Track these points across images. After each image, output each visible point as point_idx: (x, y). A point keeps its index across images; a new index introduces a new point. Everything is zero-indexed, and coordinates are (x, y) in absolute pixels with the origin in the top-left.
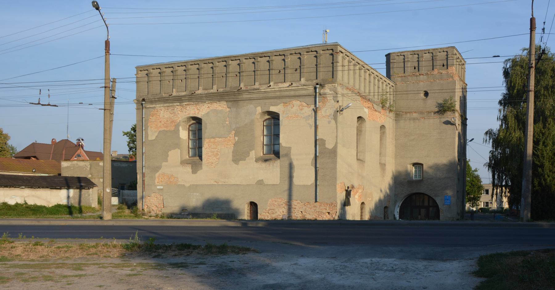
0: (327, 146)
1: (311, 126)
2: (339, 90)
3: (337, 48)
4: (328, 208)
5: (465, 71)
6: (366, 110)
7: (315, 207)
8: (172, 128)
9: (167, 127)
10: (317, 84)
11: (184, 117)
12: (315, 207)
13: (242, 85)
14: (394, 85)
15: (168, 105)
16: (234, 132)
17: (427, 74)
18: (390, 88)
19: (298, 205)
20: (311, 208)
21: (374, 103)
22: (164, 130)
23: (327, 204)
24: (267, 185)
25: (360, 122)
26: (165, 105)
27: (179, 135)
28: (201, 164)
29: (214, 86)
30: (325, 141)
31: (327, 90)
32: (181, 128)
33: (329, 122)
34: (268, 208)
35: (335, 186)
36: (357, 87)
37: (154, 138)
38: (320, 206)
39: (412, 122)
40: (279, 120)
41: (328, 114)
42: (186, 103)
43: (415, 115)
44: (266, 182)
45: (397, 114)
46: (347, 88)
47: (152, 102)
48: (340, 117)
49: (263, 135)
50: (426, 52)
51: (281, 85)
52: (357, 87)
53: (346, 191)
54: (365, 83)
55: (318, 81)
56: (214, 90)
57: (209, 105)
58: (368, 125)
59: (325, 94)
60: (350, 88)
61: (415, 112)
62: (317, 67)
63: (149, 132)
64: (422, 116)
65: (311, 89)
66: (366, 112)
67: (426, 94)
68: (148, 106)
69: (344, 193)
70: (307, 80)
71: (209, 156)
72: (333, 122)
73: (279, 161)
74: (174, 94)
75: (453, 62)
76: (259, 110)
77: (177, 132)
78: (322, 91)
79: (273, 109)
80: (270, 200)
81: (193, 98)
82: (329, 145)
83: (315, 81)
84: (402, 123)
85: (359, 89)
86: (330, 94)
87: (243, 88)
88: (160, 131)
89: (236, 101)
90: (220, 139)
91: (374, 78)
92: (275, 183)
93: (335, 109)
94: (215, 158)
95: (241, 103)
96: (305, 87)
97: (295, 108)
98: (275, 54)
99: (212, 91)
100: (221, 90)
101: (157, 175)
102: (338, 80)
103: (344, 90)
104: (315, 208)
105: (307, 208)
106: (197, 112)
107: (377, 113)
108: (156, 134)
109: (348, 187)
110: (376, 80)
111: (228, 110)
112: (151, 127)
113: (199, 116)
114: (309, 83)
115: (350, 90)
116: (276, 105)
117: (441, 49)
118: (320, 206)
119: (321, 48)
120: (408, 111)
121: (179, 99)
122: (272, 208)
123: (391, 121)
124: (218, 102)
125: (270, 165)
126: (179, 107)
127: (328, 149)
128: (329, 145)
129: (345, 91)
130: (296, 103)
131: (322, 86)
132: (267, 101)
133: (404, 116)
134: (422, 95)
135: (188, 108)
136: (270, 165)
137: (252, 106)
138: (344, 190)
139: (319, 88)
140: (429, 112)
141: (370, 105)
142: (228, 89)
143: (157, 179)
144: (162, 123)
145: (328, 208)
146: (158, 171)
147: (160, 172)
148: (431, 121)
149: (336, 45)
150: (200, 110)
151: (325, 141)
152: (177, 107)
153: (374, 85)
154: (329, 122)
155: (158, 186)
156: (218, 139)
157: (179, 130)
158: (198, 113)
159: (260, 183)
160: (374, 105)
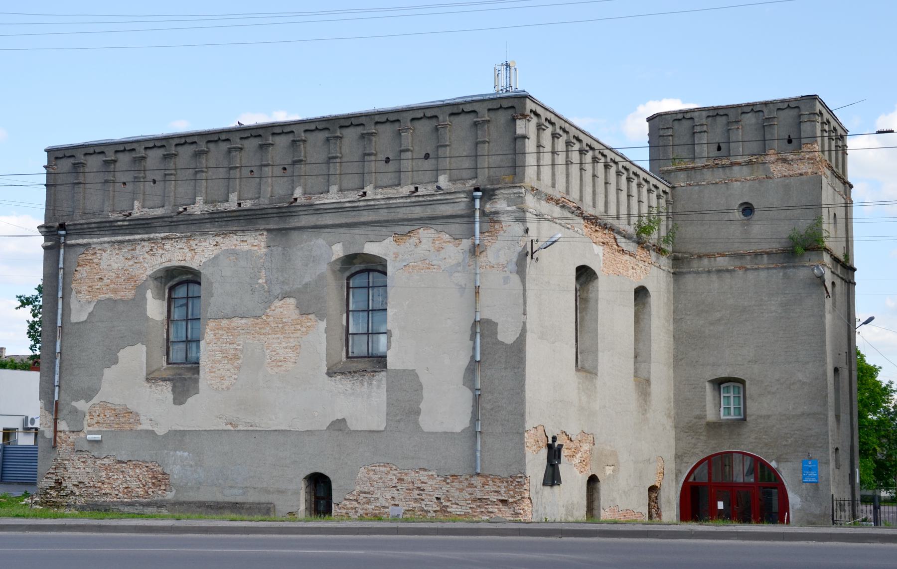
0: (501, 337)
1: (462, 288)
2: (530, 202)
3: (525, 104)
4: (503, 490)
5: (845, 153)
6: (599, 250)
7: (471, 485)
8: (130, 295)
9: (115, 291)
10: (477, 190)
11: (158, 267)
12: (471, 485)
13: (298, 193)
14: (668, 190)
15: (120, 238)
17: (749, 163)
18: (659, 197)
19: (430, 482)
21: (619, 233)
22: (109, 299)
23: (501, 480)
25: (583, 279)
26: (113, 239)
27: (145, 309)
28: (196, 381)
29: (231, 196)
30: (497, 324)
31: (501, 205)
32: (149, 294)
33: (506, 280)
34: (358, 489)
35: (521, 435)
36: (575, 194)
37: (85, 318)
38: (484, 484)
39: (714, 277)
40: (385, 273)
41: (503, 260)
42: (162, 235)
43: (722, 262)
44: (353, 425)
45: (677, 260)
46: (550, 199)
47: (81, 233)
48: (531, 268)
49: (348, 312)
50: (745, 110)
51: (391, 192)
52: (575, 194)
53: (550, 447)
54: (594, 186)
55: (482, 181)
56: (232, 205)
57: (218, 239)
58: (603, 286)
59: (496, 213)
60: (558, 196)
61: (724, 256)
62: (477, 146)
63: (74, 305)
64: (738, 263)
65: (463, 198)
66: (596, 255)
67: (748, 209)
68: (73, 242)
69: (544, 452)
70: (451, 180)
72: (515, 278)
73: (384, 373)
74: (138, 211)
75: (814, 131)
76: (339, 251)
77: (139, 301)
78: (488, 207)
79: (371, 249)
81: (181, 223)
82: (507, 336)
83: (470, 184)
84: (689, 281)
85: (581, 200)
86: (508, 212)
87: (301, 201)
88: (99, 301)
89: (283, 231)
90: (244, 321)
91: (619, 174)
93: (519, 249)
94: (229, 366)
95: (295, 235)
96: (448, 197)
97: (424, 246)
98: (377, 118)
99: (224, 206)
100: (247, 205)
102: (527, 180)
103: (543, 203)
104: (470, 490)
105: (453, 490)
106: (189, 255)
107: (627, 257)
108: (91, 308)
109: (554, 439)
110: (624, 177)
111: (264, 251)
112: (79, 292)
113: (194, 265)
114: (459, 186)
115: (557, 202)
117: (783, 101)
118: (484, 484)
119: (485, 104)
120: (703, 251)
122: (366, 489)
123: (662, 275)
125: (362, 383)
126: (146, 244)
127: (502, 343)
128: (507, 336)
129: (546, 208)
130: (427, 235)
131: (489, 195)
132: (356, 231)
133: (695, 264)
134: (738, 215)
135: (167, 246)
136: (362, 383)
137: (321, 241)
138: (543, 443)
139: (481, 198)
140: (757, 255)
141: (608, 237)
142: (264, 202)
143: (87, 417)
144: (106, 281)
145: (503, 490)
147: (95, 400)
148: (763, 274)
149: (523, 97)
150: (198, 252)
151: (497, 324)
153: (619, 190)
154: (506, 280)
155: (90, 433)
156: (237, 322)
157: (145, 299)
159: (339, 425)
160: (618, 237)
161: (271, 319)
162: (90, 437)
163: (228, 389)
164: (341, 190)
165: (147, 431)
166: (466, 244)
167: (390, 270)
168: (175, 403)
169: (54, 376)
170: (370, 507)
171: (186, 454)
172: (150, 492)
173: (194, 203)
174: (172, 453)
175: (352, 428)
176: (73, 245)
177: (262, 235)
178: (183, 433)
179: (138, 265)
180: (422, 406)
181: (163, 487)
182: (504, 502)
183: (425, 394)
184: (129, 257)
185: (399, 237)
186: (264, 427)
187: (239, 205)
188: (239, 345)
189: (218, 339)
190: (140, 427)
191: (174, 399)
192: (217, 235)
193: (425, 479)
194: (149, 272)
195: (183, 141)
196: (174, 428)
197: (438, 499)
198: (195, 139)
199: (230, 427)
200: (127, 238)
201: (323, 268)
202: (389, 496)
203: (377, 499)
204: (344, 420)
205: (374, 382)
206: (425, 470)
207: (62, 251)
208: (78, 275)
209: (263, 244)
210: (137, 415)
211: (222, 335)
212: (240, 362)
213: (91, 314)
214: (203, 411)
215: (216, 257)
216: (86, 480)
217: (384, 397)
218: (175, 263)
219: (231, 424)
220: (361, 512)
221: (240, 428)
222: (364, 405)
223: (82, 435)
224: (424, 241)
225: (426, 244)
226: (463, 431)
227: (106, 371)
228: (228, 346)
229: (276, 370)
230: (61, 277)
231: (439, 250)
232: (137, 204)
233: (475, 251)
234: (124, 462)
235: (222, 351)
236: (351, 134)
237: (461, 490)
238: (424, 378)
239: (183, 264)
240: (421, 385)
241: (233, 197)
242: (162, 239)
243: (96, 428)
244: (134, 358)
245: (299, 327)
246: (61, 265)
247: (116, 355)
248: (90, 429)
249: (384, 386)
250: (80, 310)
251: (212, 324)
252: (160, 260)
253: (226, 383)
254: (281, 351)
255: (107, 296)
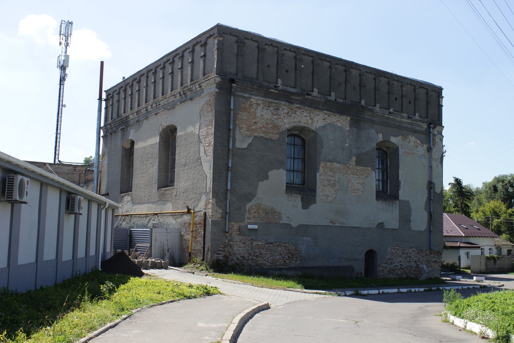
7: (427, 255)
8: (276, 137)
9: (264, 132)
10: (430, 124)
12: (427, 255)
13: (363, 102)
15: (270, 100)
16: (354, 158)
19: (414, 253)
20: (423, 257)
22: (262, 137)
24: (387, 229)
26: (267, 100)
28: (315, 196)
34: (387, 257)
37: (245, 146)
42: (297, 106)
44: (387, 226)
57: (326, 116)
63: (238, 136)
68: (238, 93)
71: (324, 186)
73: (398, 201)
80: (389, 248)
90: (338, 165)
92: (394, 228)
99: (329, 98)
100: (341, 101)
101: (248, 205)
106: (310, 121)
108: (250, 140)
111: (348, 129)
112: (241, 128)
113: (313, 128)
116: (396, 136)
118: (431, 254)
121: (286, 97)
124: (338, 116)
127: (436, 193)
130: (412, 139)
135: (298, 113)
137: (373, 131)
143: (247, 213)
146: (250, 200)
147: (253, 202)
150: (316, 120)
152: (284, 107)
156: (336, 165)
158: (312, 123)
159: (381, 225)
161: (351, 166)
162: (250, 227)
163: (331, 202)
164: (380, 107)
165: (286, 224)
166: (425, 146)
167: (400, 153)
168: (303, 208)
169: (227, 183)
170: (392, 266)
171: (309, 239)
172: (287, 261)
173: (313, 91)
174: (301, 238)
175: (386, 227)
176: (239, 96)
177: (347, 120)
178: (308, 226)
179: (281, 120)
180: (411, 218)
181: (294, 259)
182: (435, 261)
183: (412, 213)
184: (275, 113)
185: (405, 137)
186: (348, 225)
187: (336, 100)
188: (336, 178)
189: (326, 173)
190: (281, 222)
191: (303, 206)
192: (326, 114)
193: (411, 252)
194: (287, 126)
195: (306, 53)
196: (302, 223)
197: (416, 261)
198: (314, 55)
199: (331, 224)
200: (276, 101)
201: (374, 145)
202: (399, 260)
203: (394, 262)
204: (382, 223)
205: (394, 205)
206: (412, 248)
207: (232, 98)
208: (239, 116)
209: (348, 125)
210: (280, 213)
211: (328, 171)
212: (337, 188)
213: (249, 144)
214: (318, 214)
215: (325, 126)
216: (246, 255)
217: (398, 213)
218: (302, 124)
219: (332, 222)
220: (388, 269)
221: (336, 225)
222: (388, 215)
223: (243, 224)
224: (411, 141)
225: (412, 143)
226: (425, 230)
227: (260, 184)
228: (330, 178)
229: (354, 194)
230: (232, 115)
231: (416, 147)
232: (280, 81)
233: (429, 150)
234: (272, 244)
235: (328, 180)
236: (384, 80)
237: (423, 257)
238: (412, 205)
239: (306, 125)
240: (410, 210)
241: (333, 94)
242: (296, 107)
243: (253, 221)
244: (279, 177)
245: (363, 173)
246: (232, 108)
247: (267, 174)
248: (249, 221)
249: (398, 207)
250: (242, 141)
251: (322, 164)
252: (293, 120)
253: (330, 199)
254: (356, 185)
255: (261, 135)
